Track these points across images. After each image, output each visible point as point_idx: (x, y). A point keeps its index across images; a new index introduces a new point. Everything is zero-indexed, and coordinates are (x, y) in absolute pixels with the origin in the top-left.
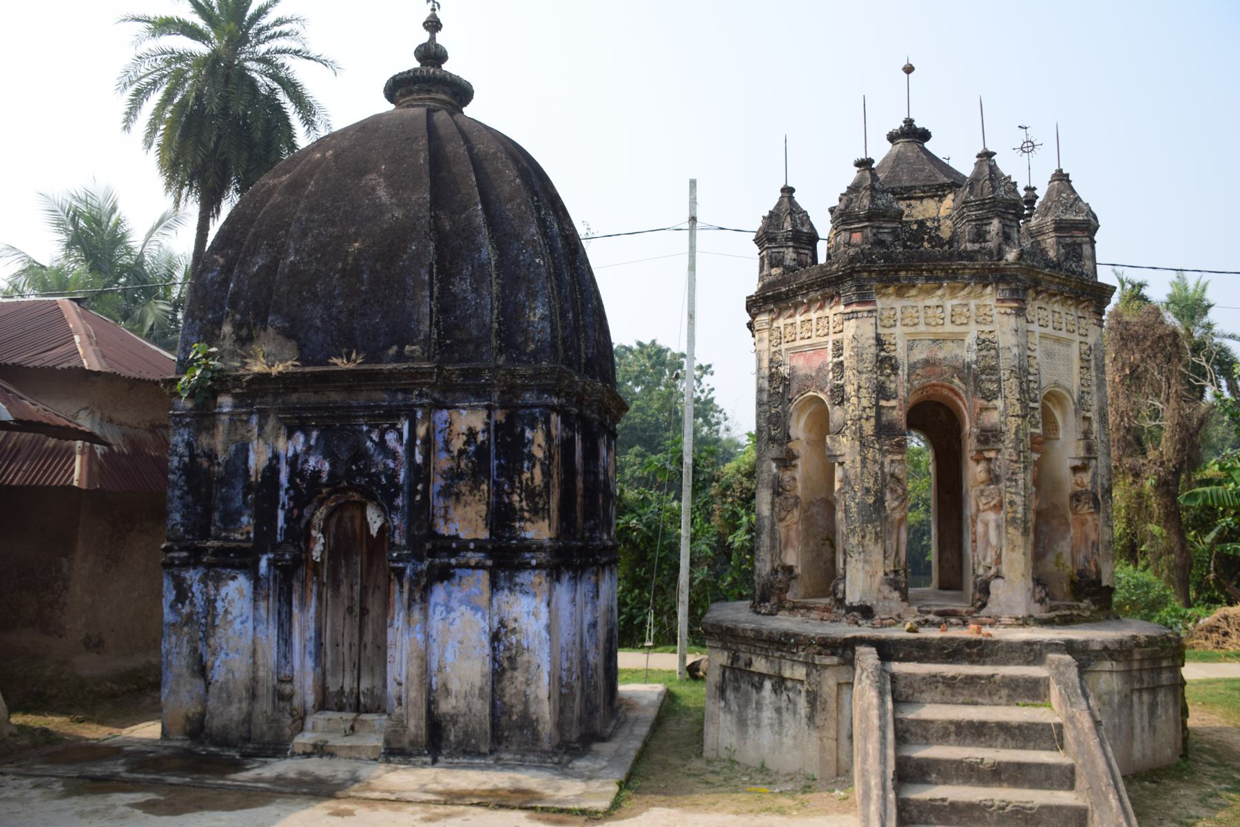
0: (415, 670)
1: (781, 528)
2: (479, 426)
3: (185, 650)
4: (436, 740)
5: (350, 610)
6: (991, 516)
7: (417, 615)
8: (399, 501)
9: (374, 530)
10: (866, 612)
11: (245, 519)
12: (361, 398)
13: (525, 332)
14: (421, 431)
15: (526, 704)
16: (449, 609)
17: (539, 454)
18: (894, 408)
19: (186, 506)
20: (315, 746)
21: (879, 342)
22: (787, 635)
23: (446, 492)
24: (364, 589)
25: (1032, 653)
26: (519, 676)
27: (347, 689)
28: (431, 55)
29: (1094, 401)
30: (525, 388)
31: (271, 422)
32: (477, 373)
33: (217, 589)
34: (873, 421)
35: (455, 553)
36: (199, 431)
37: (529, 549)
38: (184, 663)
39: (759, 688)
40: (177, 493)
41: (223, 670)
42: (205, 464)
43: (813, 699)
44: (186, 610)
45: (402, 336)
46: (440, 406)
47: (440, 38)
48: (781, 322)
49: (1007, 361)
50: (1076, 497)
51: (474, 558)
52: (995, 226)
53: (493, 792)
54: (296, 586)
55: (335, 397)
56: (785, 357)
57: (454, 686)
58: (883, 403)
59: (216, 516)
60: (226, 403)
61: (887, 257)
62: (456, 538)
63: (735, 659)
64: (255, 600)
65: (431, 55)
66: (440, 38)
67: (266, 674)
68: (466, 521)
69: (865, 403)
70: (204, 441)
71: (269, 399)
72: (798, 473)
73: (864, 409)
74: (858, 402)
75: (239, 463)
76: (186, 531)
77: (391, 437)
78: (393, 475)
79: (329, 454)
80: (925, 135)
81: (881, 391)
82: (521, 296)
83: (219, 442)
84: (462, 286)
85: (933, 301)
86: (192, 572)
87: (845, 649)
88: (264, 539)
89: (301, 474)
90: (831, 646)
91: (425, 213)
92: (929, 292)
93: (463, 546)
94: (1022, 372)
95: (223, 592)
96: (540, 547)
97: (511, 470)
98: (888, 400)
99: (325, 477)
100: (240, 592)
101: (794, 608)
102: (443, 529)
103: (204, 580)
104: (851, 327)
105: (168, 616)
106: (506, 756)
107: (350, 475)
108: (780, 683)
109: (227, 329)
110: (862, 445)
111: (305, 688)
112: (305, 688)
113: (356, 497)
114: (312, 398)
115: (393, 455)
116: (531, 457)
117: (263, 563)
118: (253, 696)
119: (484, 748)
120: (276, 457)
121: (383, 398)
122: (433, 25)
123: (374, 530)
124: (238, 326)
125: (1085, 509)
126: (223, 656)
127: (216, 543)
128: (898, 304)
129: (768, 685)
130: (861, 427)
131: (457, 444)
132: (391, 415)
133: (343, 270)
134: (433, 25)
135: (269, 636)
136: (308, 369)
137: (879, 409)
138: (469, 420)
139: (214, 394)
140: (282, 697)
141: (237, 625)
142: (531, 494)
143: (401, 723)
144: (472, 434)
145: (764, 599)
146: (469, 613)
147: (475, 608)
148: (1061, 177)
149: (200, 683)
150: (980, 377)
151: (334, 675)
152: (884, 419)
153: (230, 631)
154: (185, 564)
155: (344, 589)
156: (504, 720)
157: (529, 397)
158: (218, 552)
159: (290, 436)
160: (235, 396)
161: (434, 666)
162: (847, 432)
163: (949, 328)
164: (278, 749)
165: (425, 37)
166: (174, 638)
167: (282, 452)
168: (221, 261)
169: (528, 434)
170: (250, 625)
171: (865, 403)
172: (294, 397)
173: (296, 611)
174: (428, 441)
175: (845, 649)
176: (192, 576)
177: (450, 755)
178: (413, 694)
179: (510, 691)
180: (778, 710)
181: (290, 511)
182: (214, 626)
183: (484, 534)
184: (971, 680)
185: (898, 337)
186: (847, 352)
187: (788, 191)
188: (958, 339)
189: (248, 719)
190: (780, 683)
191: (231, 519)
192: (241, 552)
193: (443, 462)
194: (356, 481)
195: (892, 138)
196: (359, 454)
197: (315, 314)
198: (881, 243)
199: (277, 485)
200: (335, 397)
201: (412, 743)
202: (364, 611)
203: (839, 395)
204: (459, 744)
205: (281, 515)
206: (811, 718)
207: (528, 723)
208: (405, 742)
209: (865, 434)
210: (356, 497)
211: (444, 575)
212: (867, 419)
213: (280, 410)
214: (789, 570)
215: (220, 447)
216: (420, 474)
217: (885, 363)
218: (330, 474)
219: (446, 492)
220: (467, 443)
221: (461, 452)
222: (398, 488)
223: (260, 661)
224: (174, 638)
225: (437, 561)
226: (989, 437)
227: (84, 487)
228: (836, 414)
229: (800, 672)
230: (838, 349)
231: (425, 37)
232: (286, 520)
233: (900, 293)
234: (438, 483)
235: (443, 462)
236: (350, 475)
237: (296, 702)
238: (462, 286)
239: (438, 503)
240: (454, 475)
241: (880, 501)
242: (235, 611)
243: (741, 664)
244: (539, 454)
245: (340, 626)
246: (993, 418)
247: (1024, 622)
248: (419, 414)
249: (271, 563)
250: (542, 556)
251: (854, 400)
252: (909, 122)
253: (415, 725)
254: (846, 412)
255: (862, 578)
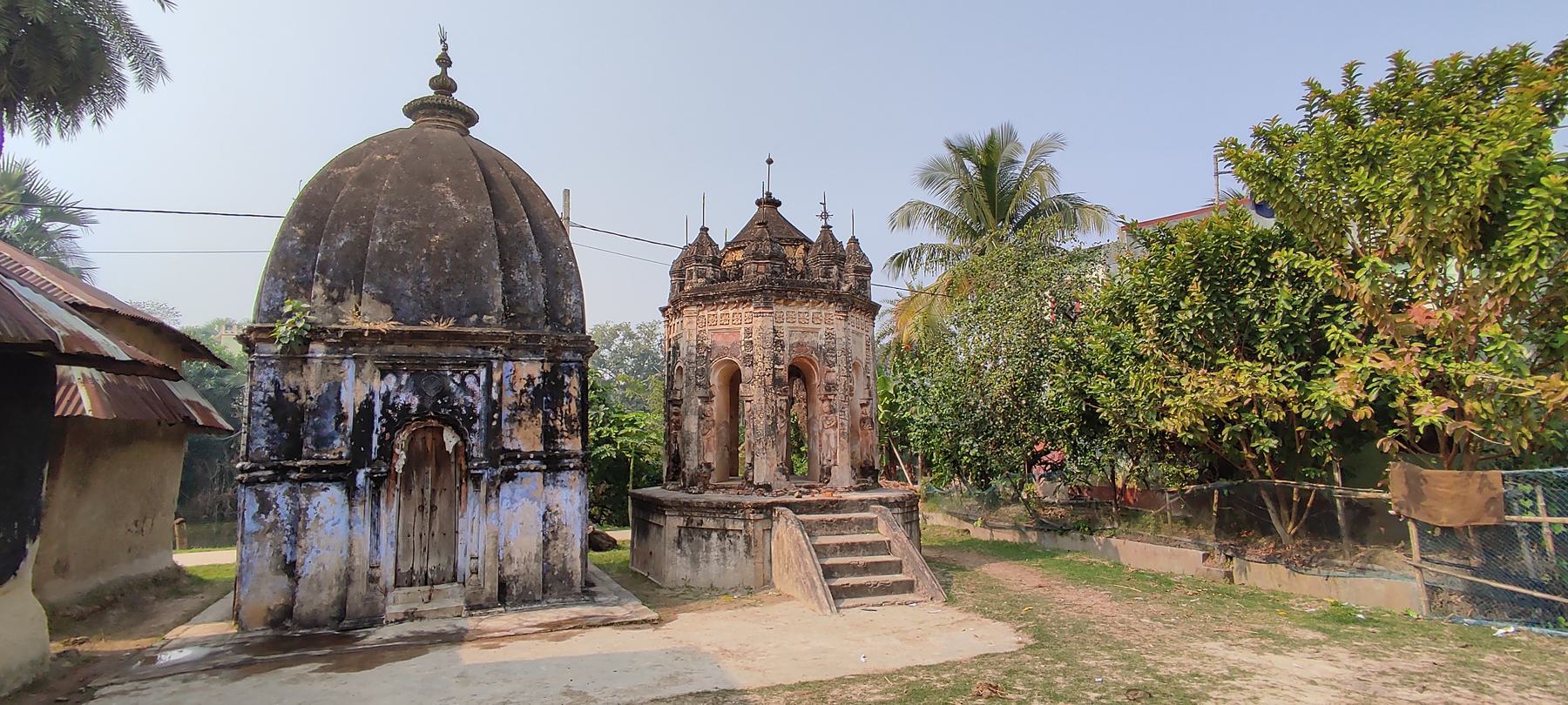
0: (490, 546)
1: (704, 440)
2: (536, 374)
3: (269, 552)
4: (505, 595)
5: (422, 508)
6: (832, 431)
7: (492, 506)
8: (476, 426)
9: (449, 448)
10: (768, 488)
11: (337, 442)
12: (447, 351)
13: (564, 311)
14: (496, 376)
15: (564, 563)
16: (513, 501)
17: (575, 393)
19: (271, 433)
20: (406, 613)
21: (775, 332)
22: (731, 504)
23: (511, 419)
24: (433, 491)
25: (863, 505)
26: (560, 544)
27: (416, 569)
28: (444, 86)
29: (871, 367)
30: (565, 349)
31: (369, 365)
32: (538, 337)
33: (308, 499)
35: (518, 461)
36: (285, 371)
37: (568, 457)
38: (267, 564)
39: (708, 538)
40: (262, 422)
41: (314, 565)
42: (292, 398)
43: (748, 540)
44: (271, 518)
45: (481, 309)
46: (507, 359)
47: (451, 72)
48: (706, 313)
49: (839, 346)
50: (863, 420)
51: (533, 464)
52: (835, 269)
53: (572, 620)
54: (383, 491)
55: (426, 350)
56: (708, 335)
57: (516, 555)
59: (309, 440)
60: (318, 350)
61: (780, 282)
62: (519, 451)
63: (690, 521)
64: (351, 506)
65: (444, 86)
66: (451, 72)
67: (361, 564)
68: (525, 438)
70: (291, 379)
71: (366, 348)
72: (714, 406)
74: (763, 365)
75: (332, 397)
76: (271, 454)
77: (470, 380)
78: (471, 408)
79: (418, 391)
80: (779, 204)
81: (776, 360)
82: (560, 287)
83: (311, 381)
84: (520, 276)
85: (803, 310)
86: (276, 486)
87: (767, 510)
88: (359, 455)
89: (393, 407)
90: (758, 508)
91: (490, 219)
92: (801, 304)
93: (526, 456)
94: (846, 352)
95: (315, 501)
96: (576, 456)
97: (555, 404)
99: (414, 410)
100: (333, 500)
101: (715, 489)
102: (508, 445)
103: (292, 493)
104: (758, 322)
105: (250, 526)
106: (552, 601)
107: (436, 407)
108: (724, 532)
109: (317, 290)
111: (387, 575)
112: (387, 575)
113: (435, 423)
114: (404, 349)
115: (473, 394)
116: (569, 395)
117: (361, 476)
118: (348, 580)
119: (538, 597)
120: (372, 393)
121: (468, 353)
122: (444, 61)
123: (449, 448)
124: (329, 289)
125: (868, 426)
126: (314, 552)
127: (309, 463)
128: (785, 310)
129: (714, 535)
131: (520, 386)
132: (473, 364)
133: (428, 255)
134: (444, 61)
135: (363, 532)
136: (407, 328)
138: (530, 369)
139: (307, 342)
140: (373, 579)
141: (328, 527)
142: (569, 420)
143: (479, 587)
144: (530, 379)
145: (693, 484)
146: (528, 503)
147: (533, 499)
148: (854, 240)
149: (284, 580)
150: (826, 353)
151: (405, 559)
153: (322, 533)
154: (270, 481)
155: (415, 493)
156: (548, 575)
157: (567, 355)
158: (308, 469)
159: (382, 378)
160: (329, 344)
161: (501, 542)
163: (811, 325)
164: (375, 620)
165: (438, 71)
166: (256, 544)
167: (376, 390)
168: (300, 232)
169: (567, 380)
170: (343, 525)
172: (389, 349)
173: (383, 511)
174: (500, 384)
175: (767, 510)
176: (278, 492)
177: (513, 605)
178: (489, 564)
179: (553, 554)
180: (723, 550)
181: (383, 434)
182: (305, 530)
183: (541, 448)
184: (840, 521)
185: (785, 328)
186: (755, 336)
187: (704, 229)
188: (815, 331)
189: (342, 601)
190: (724, 532)
191: (322, 442)
192: (333, 468)
193: (509, 398)
194: (442, 411)
195: (759, 203)
196: (444, 392)
197: (406, 285)
198: (775, 273)
199: (373, 415)
200: (426, 350)
201: (488, 600)
202: (433, 508)
203: (750, 360)
204: (519, 596)
205: (375, 437)
206: (748, 552)
207: (566, 575)
208: (482, 601)
210: (435, 423)
211: (509, 477)
213: (377, 358)
214: (708, 465)
215: (312, 385)
216: (494, 406)
217: (778, 343)
218: (419, 407)
219: (511, 419)
220: (527, 385)
221: (522, 392)
222: (476, 417)
223: (356, 553)
224: (256, 544)
225: (507, 465)
226: (831, 387)
227: (101, 416)
228: (746, 372)
229: (740, 525)
230: (749, 333)
231: (438, 71)
232: (380, 442)
233: (786, 304)
234: (506, 412)
235: (509, 398)
236: (436, 407)
237: (381, 583)
238: (520, 276)
239: (506, 427)
240: (518, 408)
241: (775, 423)
242: (326, 516)
243: (694, 524)
244: (575, 393)
245: (417, 522)
246: (832, 377)
247: (849, 490)
248: (495, 365)
249: (368, 476)
250: (577, 462)
252: (769, 195)
253: (491, 587)
255: (765, 469)
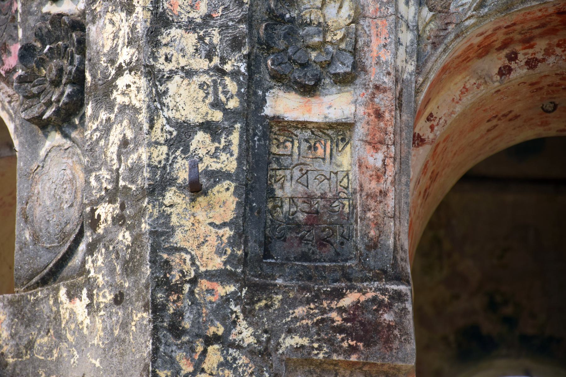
18: (340, 131)
34: (225, 200)
58: (284, 104)
69: (187, 101)
73: (183, 132)
98: (309, 90)
110: (167, 327)
130: (162, 233)
137: (262, 139)
152: (287, 189)
162: (96, 265)
171: (187, 101)
209: (181, 265)
212: (196, 189)
251: (131, 89)
254: (93, 158)
